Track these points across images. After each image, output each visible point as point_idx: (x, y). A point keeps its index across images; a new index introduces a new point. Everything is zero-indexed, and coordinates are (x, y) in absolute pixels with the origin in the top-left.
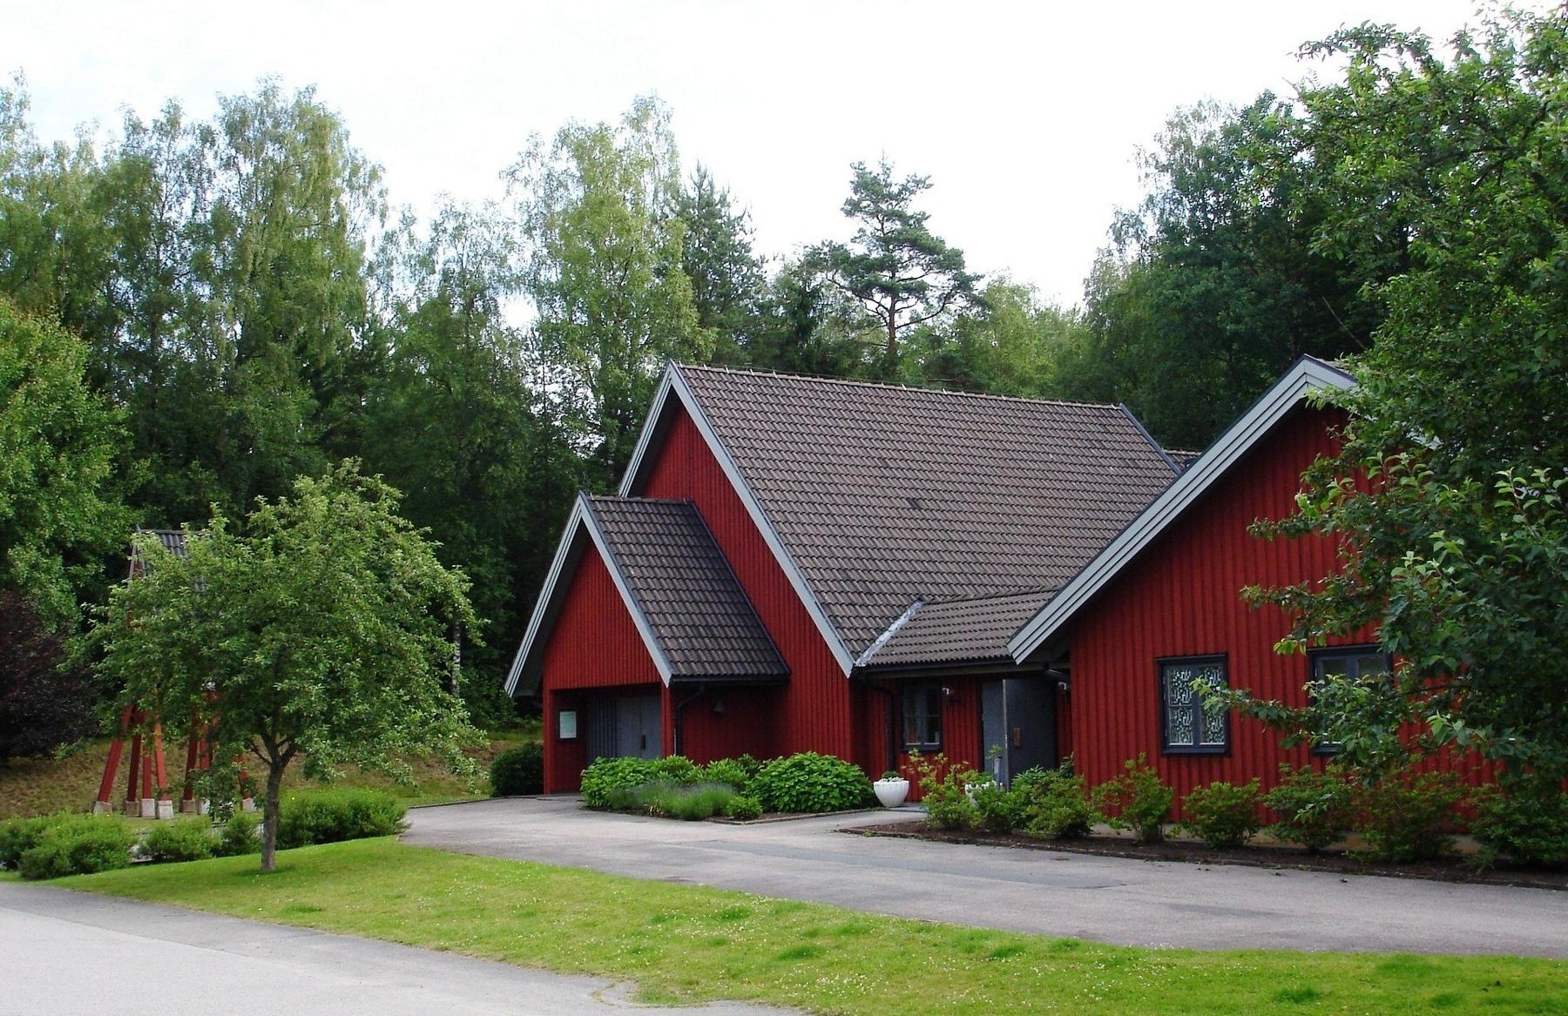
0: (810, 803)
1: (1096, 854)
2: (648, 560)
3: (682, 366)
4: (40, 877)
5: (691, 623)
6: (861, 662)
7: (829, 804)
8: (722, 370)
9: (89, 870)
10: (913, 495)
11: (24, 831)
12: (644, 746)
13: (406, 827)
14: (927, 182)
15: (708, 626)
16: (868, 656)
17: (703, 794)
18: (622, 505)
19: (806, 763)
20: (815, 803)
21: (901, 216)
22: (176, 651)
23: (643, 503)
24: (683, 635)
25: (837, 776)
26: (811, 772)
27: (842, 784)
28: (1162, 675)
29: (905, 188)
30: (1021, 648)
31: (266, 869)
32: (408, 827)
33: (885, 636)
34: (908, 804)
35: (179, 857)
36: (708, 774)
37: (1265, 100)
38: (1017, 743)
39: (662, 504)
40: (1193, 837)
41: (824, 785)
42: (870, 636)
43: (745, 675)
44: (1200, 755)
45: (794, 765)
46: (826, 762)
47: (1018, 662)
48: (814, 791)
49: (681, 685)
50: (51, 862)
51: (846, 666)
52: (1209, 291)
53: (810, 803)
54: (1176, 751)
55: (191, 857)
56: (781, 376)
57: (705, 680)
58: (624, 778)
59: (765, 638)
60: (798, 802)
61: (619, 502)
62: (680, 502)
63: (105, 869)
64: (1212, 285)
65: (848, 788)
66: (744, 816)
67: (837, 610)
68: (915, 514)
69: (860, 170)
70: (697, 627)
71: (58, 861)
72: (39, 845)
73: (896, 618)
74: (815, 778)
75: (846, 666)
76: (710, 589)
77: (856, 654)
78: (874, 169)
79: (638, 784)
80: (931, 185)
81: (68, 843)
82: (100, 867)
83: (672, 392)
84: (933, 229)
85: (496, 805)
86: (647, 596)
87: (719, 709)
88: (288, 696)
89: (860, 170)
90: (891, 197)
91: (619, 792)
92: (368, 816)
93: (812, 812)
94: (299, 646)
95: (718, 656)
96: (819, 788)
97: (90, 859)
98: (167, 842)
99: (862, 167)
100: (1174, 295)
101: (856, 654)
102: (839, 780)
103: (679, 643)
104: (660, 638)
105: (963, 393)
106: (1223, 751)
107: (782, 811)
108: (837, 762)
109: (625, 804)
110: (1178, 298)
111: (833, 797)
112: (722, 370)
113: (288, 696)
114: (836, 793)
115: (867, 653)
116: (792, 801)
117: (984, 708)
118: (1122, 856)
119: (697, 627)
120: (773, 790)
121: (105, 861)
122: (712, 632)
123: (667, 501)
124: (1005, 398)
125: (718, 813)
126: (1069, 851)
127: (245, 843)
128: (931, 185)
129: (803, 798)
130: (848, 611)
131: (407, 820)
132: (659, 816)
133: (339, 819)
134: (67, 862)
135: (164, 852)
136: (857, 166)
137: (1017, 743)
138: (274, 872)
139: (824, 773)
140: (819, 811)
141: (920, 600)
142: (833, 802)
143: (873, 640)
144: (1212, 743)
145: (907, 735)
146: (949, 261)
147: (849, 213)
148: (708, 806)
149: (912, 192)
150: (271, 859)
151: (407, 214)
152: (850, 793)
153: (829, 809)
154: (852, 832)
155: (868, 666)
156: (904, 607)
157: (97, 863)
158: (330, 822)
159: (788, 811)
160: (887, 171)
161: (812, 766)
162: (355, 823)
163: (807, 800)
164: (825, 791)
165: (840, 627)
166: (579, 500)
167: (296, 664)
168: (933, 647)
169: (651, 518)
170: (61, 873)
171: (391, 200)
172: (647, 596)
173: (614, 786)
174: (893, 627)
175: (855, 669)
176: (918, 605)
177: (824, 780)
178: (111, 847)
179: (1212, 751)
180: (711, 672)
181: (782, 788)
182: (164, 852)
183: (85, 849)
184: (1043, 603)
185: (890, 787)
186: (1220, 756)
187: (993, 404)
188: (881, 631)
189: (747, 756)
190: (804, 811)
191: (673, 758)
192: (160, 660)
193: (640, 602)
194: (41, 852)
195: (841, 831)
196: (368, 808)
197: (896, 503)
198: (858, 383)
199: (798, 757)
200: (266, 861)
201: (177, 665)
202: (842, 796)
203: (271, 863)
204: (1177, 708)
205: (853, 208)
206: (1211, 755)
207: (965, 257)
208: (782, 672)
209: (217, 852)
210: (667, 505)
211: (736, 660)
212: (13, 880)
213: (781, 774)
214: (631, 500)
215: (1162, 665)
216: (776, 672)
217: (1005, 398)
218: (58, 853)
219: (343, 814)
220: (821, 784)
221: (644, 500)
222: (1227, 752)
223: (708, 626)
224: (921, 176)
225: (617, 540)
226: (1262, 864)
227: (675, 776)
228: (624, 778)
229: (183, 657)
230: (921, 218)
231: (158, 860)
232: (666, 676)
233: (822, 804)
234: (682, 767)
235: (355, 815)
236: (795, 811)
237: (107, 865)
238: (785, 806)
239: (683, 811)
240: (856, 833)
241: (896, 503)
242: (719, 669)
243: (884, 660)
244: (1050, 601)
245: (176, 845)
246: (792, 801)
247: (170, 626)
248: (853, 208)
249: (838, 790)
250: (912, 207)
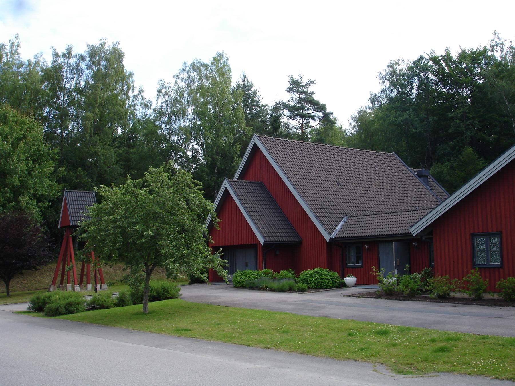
0: (322, 286)
1: (463, 304)
2: (251, 201)
3: (258, 136)
4: (53, 315)
5: (268, 223)
6: (333, 236)
7: (329, 286)
8: (271, 137)
9: (71, 312)
10: (337, 180)
11: (42, 297)
12: (247, 266)
13: (180, 295)
14: (315, 82)
15: (273, 224)
16: (334, 234)
17: (285, 283)
18: (240, 183)
19: (319, 271)
20: (324, 286)
21: (305, 93)
22: (119, 230)
23: (246, 182)
24: (266, 227)
25: (331, 276)
26: (322, 275)
27: (333, 279)
28: (473, 239)
29: (307, 84)
30: (415, 230)
31: (145, 312)
32: (181, 295)
33: (338, 228)
35: (103, 307)
36: (280, 275)
37: (421, 58)
38: (398, 264)
39: (252, 183)
40: (499, 297)
41: (327, 279)
42: (334, 228)
43: (292, 241)
44: (489, 268)
45: (315, 272)
46: (326, 271)
47: (414, 235)
48: (323, 281)
49: (267, 245)
50: (57, 309)
51: (327, 239)
52: (407, 119)
53: (322, 286)
54: (492, 266)
55: (107, 307)
56: (290, 140)
57: (274, 243)
58: (249, 277)
59: (292, 228)
60: (317, 285)
62: (258, 182)
63: (77, 312)
64: (408, 117)
65: (335, 280)
66: (301, 290)
67: (322, 219)
68: (339, 186)
70: (270, 225)
71: (60, 310)
72: (50, 303)
73: (340, 222)
74: (324, 276)
75: (327, 239)
76: (272, 212)
77: (330, 234)
78: (296, 78)
79: (255, 279)
80: (316, 83)
81: (63, 302)
82: (75, 311)
83: (255, 144)
84: (316, 97)
85: (197, 286)
86: (252, 214)
87: (278, 253)
88: (162, 247)
90: (302, 86)
91: (248, 282)
92: (168, 291)
93: (322, 289)
94: (163, 229)
95: (278, 234)
96: (325, 280)
97: (71, 308)
98: (99, 302)
99: (292, 77)
100: (395, 120)
101: (330, 234)
102: (332, 278)
103: (265, 230)
104: (258, 228)
105: (346, 148)
106: (500, 266)
107: (311, 288)
108: (329, 271)
109: (251, 286)
110: (396, 121)
111: (330, 283)
112: (271, 137)
113: (162, 247)
114: (331, 282)
115: (333, 233)
116: (315, 285)
117: (380, 253)
118: (474, 305)
119: (270, 225)
120: (307, 281)
121: (77, 309)
122: (275, 226)
123: (254, 182)
124: (359, 150)
125: (291, 290)
126: (451, 303)
127: (125, 302)
128: (316, 83)
129: (319, 284)
130: (325, 219)
131: (180, 292)
132: (266, 290)
133: (158, 293)
134: (64, 310)
135: (96, 305)
136: (290, 76)
137: (398, 264)
138: (148, 314)
139: (326, 275)
140: (325, 289)
141: (346, 215)
142: (330, 285)
143: (335, 229)
144: (494, 264)
145: (348, 262)
146: (321, 108)
147: (289, 92)
148: (287, 287)
149: (310, 85)
150: (147, 308)
151: (141, 89)
152: (336, 282)
153: (329, 288)
154: (352, 296)
155: (335, 238)
156: (342, 218)
157: (74, 310)
158: (155, 294)
159: (314, 289)
160: (301, 78)
161: (322, 273)
162: (163, 294)
163: (321, 285)
164: (327, 281)
165: (323, 225)
166: (225, 181)
167: (162, 235)
168: (360, 231)
169: (249, 188)
170: (60, 314)
171: (135, 84)
172: (252, 214)
173: (246, 280)
174: (340, 225)
175: (331, 239)
176: (346, 217)
177: (327, 278)
178: (79, 303)
179: (494, 266)
180: (277, 240)
181: (311, 280)
182: (96, 305)
183: (69, 304)
184: (426, 214)
185: (350, 280)
186: (499, 268)
187: (355, 151)
188: (337, 226)
189: (290, 269)
190: (320, 288)
191: (266, 270)
192: (113, 233)
193: (250, 216)
194: (54, 306)
195: (347, 296)
196: (168, 288)
197: (333, 183)
198: (314, 143)
199: (316, 269)
200: (145, 308)
201: (119, 235)
202: (333, 283)
203: (147, 310)
204: (479, 251)
205: (290, 90)
206: (494, 268)
207: (327, 106)
208: (299, 240)
209: (117, 305)
210: (254, 183)
211: (284, 236)
212: (42, 316)
213: (311, 275)
214: (239, 181)
215: (473, 236)
216: (297, 240)
217: (359, 150)
218: (60, 306)
219: (159, 291)
220: (326, 279)
221: (242, 181)
222: (502, 266)
223: (273, 224)
224: (313, 80)
225: (240, 195)
226: (495, 305)
227: (268, 276)
228: (249, 277)
229: (120, 233)
230: (313, 93)
231: (94, 308)
232: (262, 241)
233: (326, 286)
234: (269, 273)
235: (163, 291)
236: (316, 288)
237: (78, 311)
238: (313, 286)
239: (278, 289)
240: (354, 296)
241: (333, 183)
242: (279, 239)
243: (340, 236)
244: (429, 213)
245: (102, 303)
246: (315, 285)
247: (117, 220)
248: (290, 90)
249: (331, 281)
250: (310, 90)
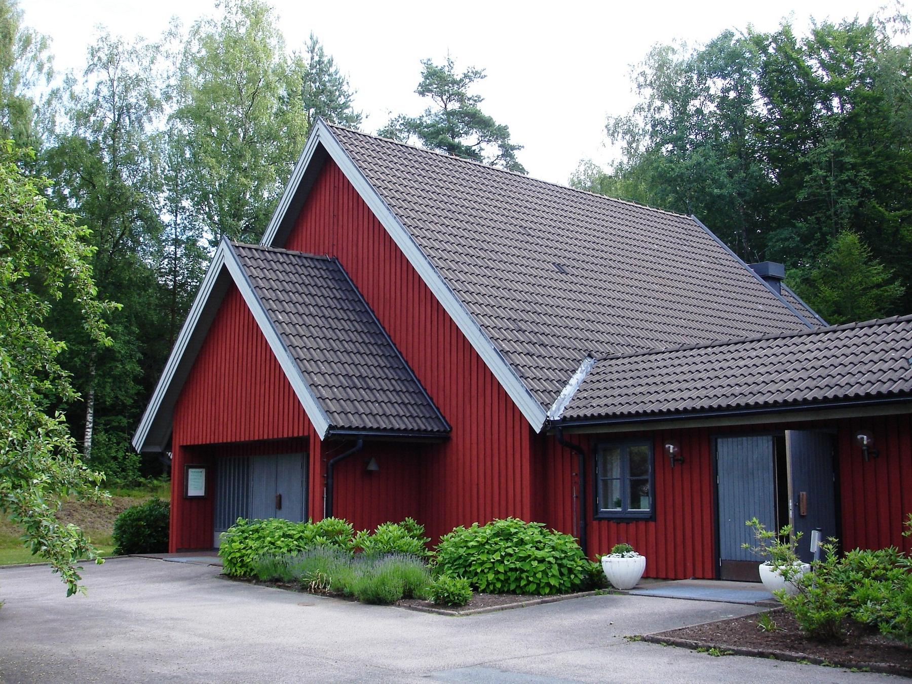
0: (523, 583)
5: (344, 373)
6: (556, 412)
7: (548, 584)
12: (279, 506)
14: (483, 74)
20: (529, 582)
21: (461, 98)
23: (287, 255)
25: (554, 548)
26: (522, 542)
27: (561, 559)
29: (466, 76)
33: (568, 391)
34: (651, 583)
36: (376, 542)
37: (727, 36)
38: (803, 511)
41: (542, 561)
42: (555, 390)
45: (497, 535)
48: (527, 568)
52: (699, 164)
53: (523, 583)
58: (273, 544)
61: (263, 251)
62: (324, 258)
64: (702, 160)
67: (518, 359)
68: (563, 277)
69: (428, 65)
73: (574, 371)
74: (529, 549)
77: (547, 406)
78: (439, 63)
79: (290, 551)
80: (485, 76)
84: (486, 109)
86: (296, 342)
87: (373, 467)
89: (428, 65)
90: (454, 82)
91: (268, 561)
95: (376, 408)
96: (535, 563)
99: (429, 63)
100: (670, 167)
103: (333, 393)
107: (484, 591)
108: (545, 531)
109: (276, 575)
110: (673, 169)
111: (553, 576)
114: (555, 570)
116: (498, 579)
120: (470, 565)
123: (311, 255)
128: (485, 76)
130: (528, 360)
132: (324, 594)
136: (425, 61)
140: (532, 594)
141: (590, 356)
142: (553, 582)
143: (558, 392)
145: (600, 500)
146: (500, 134)
147: (422, 93)
148: (396, 586)
149: (471, 80)
151: (70, 76)
152: (570, 571)
155: (564, 419)
159: (492, 592)
160: (451, 64)
161: (521, 535)
163: (518, 579)
164: (542, 567)
171: (57, 66)
172: (296, 342)
173: (261, 552)
174: (573, 381)
177: (539, 554)
180: (370, 425)
187: (598, 199)
188: (565, 383)
189: (410, 521)
191: (330, 523)
195: (644, 640)
199: (501, 524)
202: (562, 574)
205: (424, 90)
207: (510, 130)
210: (312, 259)
213: (482, 545)
220: (535, 559)
224: (478, 69)
227: (335, 542)
228: (273, 544)
230: (479, 99)
232: (321, 426)
233: (538, 585)
234: (340, 532)
236: (501, 592)
238: (488, 584)
239: (364, 591)
242: (378, 423)
248: (424, 90)
249: (556, 567)
250: (471, 90)
